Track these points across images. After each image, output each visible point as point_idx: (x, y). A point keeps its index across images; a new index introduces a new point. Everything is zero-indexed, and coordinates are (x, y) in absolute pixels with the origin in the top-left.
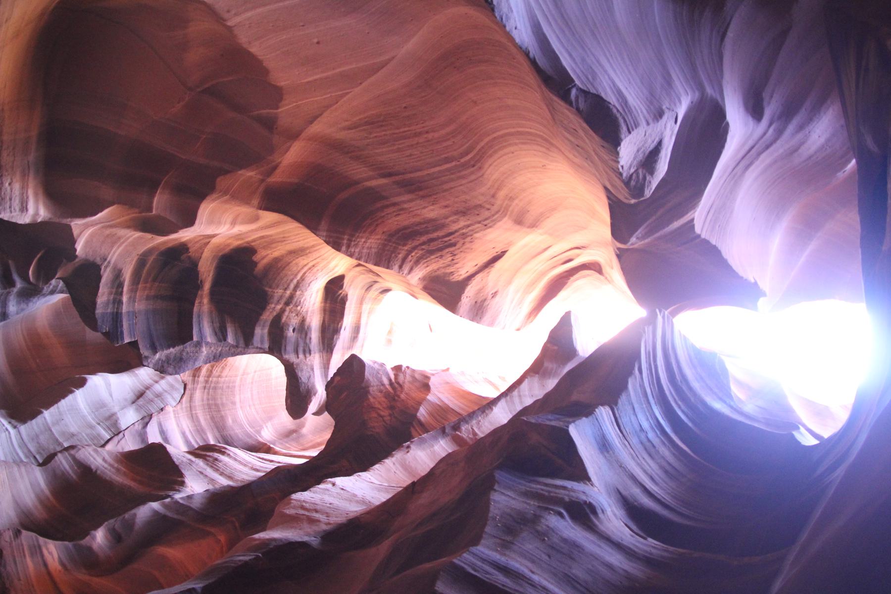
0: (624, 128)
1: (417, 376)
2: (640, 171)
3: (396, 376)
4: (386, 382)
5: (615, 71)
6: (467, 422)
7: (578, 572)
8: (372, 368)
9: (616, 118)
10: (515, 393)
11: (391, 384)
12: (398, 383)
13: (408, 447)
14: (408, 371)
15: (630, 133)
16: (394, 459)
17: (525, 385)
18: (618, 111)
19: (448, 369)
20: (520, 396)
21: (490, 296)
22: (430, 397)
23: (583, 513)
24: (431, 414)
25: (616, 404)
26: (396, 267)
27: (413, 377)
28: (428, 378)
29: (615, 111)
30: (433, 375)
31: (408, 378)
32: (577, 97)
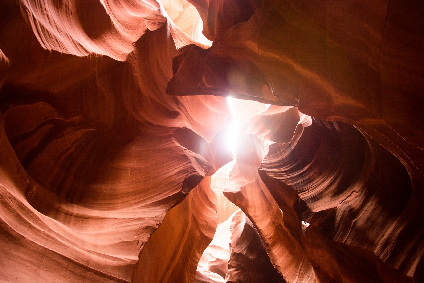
0: (195, 173)
1: (233, 258)
2: (203, 167)
3: (233, 267)
4: (236, 272)
5: (168, 172)
6: (266, 240)
7: (380, 220)
8: (230, 278)
9: (191, 176)
10: (254, 219)
11: (237, 270)
12: (237, 267)
13: (276, 266)
14: (231, 262)
15: (196, 171)
16: (283, 273)
17: (251, 214)
18: (188, 175)
19: (230, 244)
20: (255, 217)
21: (206, 223)
22: (244, 253)
23: (352, 213)
24: (252, 254)
25: (297, 191)
26: (196, 264)
27: (234, 260)
28: (235, 253)
29: (188, 176)
30: (233, 251)
31: (234, 262)
32: (185, 191)
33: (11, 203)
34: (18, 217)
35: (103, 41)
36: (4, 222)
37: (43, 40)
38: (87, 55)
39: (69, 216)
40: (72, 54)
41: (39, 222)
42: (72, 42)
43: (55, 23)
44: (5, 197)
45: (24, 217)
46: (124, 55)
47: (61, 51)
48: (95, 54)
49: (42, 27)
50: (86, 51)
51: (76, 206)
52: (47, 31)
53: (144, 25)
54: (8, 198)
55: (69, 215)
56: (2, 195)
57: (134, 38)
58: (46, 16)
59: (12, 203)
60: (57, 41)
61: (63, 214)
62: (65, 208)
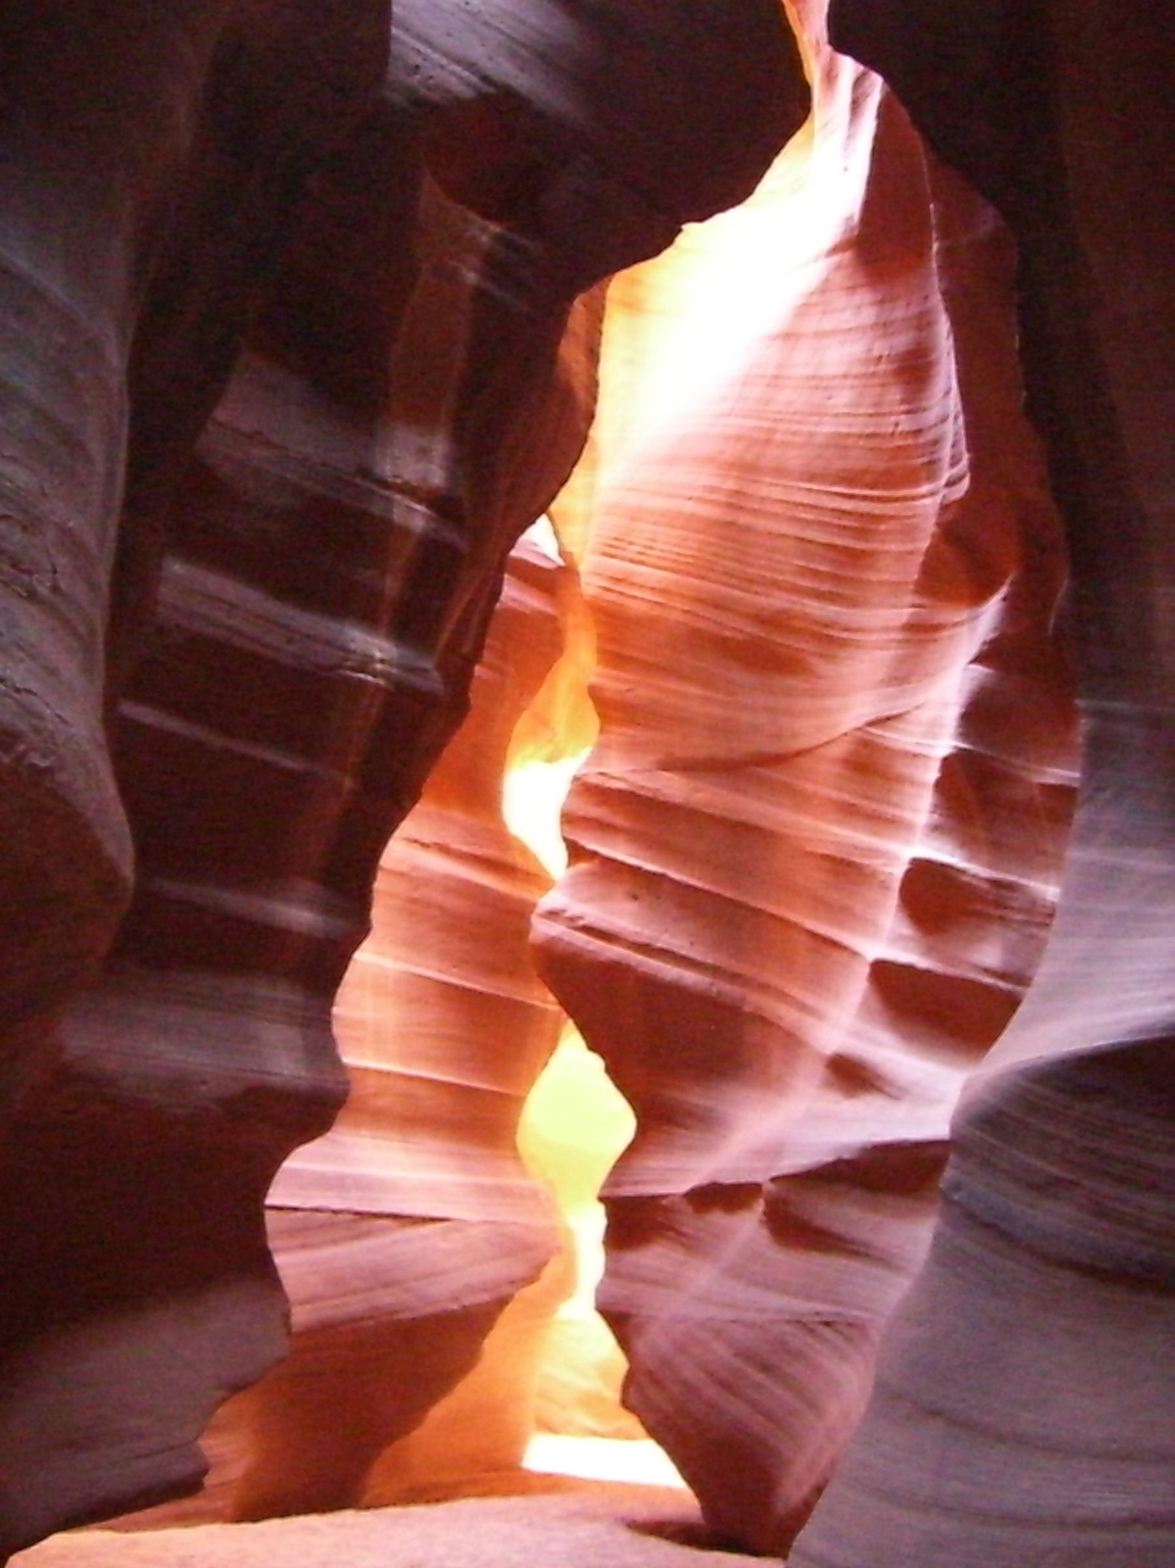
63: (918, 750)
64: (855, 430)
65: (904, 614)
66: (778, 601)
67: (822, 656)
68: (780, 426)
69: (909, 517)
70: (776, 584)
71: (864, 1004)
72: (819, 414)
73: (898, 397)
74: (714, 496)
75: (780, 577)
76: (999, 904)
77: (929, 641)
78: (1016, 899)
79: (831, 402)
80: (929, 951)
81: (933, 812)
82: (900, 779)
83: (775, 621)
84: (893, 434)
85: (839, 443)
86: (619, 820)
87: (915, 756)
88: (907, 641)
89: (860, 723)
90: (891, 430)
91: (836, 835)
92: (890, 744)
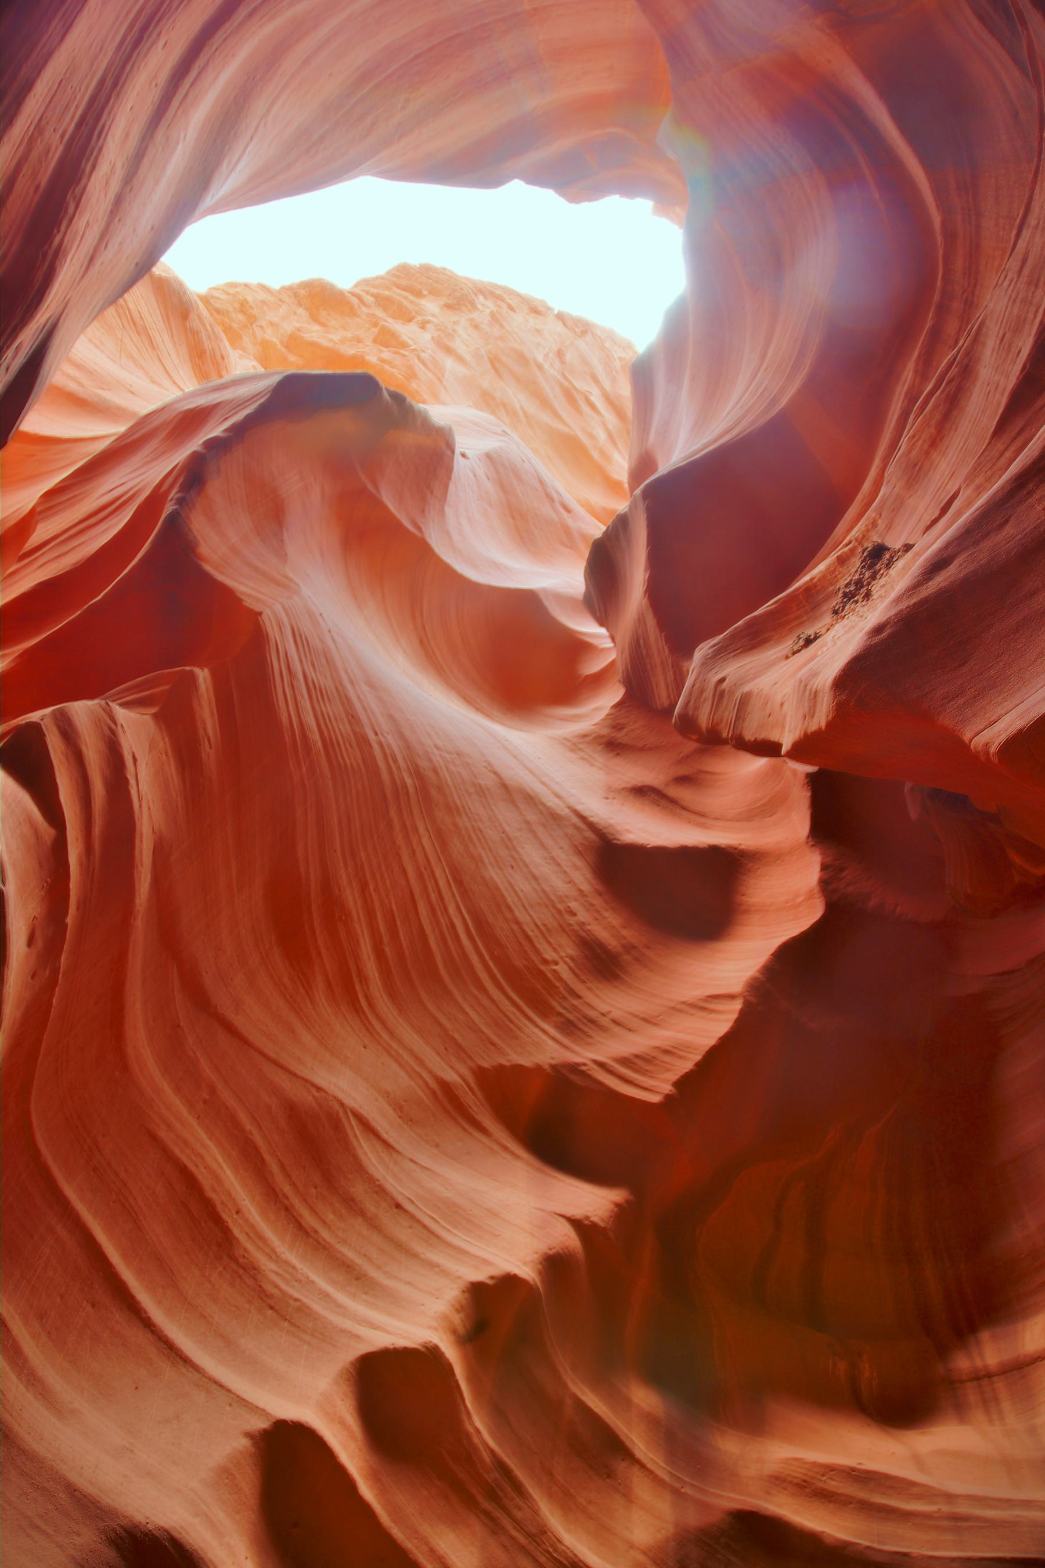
33: (834, 1485)
34: (866, 1508)
35: (746, 912)
36: (846, 1544)
37: (645, 1085)
38: (737, 1005)
39: (985, 1382)
40: (712, 1041)
41: (915, 1490)
42: (693, 1011)
43: (636, 1016)
44: (814, 1478)
45: (878, 1499)
46: (810, 896)
47: (687, 1066)
48: (754, 979)
49: (624, 1061)
50: (732, 997)
51: (985, 1335)
52: (637, 1056)
53: (794, 772)
54: (819, 1477)
55: (982, 1377)
56: (805, 1478)
57: (797, 823)
58: (612, 1026)
59: (833, 1483)
60: (666, 1052)
61: (969, 1384)
62: (962, 1363)
63: (409, 1207)
64: (517, 914)
65: (451, 1076)
66: (351, 898)
67: (329, 984)
68: (466, 819)
69: (511, 1021)
70: (364, 887)
71: (225, 1474)
72: (496, 861)
73: (571, 952)
74: (391, 762)
75: (372, 887)
76: (493, 1495)
77: (459, 1124)
78: (520, 1509)
79: (510, 869)
80: (375, 1477)
81: (458, 1311)
82: (352, 1205)
83: (333, 909)
84: (546, 962)
85: (499, 903)
86: (97, 830)
87: (398, 1206)
88: (434, 1093)
89: (349, 1102)
90: (547, 957)
91: (222, 1168)
92: (360, 1152)
